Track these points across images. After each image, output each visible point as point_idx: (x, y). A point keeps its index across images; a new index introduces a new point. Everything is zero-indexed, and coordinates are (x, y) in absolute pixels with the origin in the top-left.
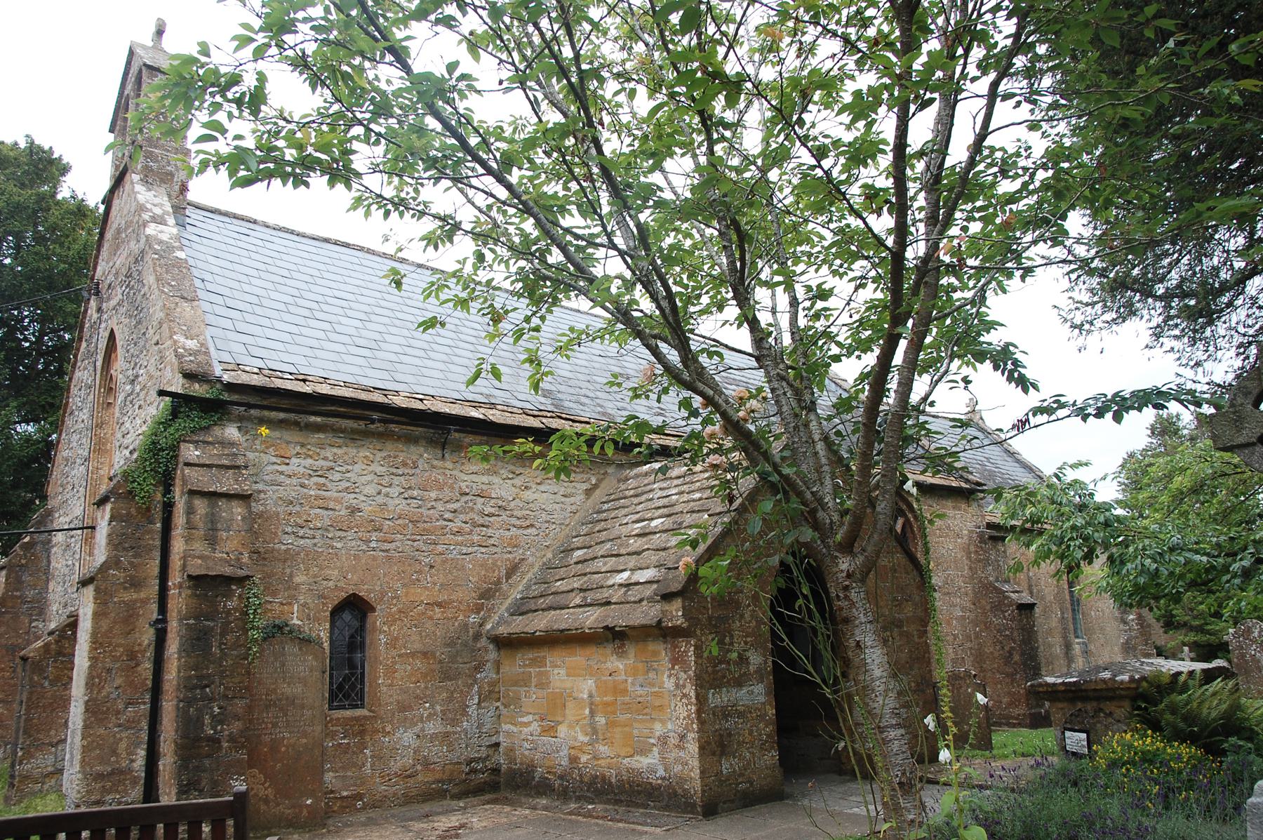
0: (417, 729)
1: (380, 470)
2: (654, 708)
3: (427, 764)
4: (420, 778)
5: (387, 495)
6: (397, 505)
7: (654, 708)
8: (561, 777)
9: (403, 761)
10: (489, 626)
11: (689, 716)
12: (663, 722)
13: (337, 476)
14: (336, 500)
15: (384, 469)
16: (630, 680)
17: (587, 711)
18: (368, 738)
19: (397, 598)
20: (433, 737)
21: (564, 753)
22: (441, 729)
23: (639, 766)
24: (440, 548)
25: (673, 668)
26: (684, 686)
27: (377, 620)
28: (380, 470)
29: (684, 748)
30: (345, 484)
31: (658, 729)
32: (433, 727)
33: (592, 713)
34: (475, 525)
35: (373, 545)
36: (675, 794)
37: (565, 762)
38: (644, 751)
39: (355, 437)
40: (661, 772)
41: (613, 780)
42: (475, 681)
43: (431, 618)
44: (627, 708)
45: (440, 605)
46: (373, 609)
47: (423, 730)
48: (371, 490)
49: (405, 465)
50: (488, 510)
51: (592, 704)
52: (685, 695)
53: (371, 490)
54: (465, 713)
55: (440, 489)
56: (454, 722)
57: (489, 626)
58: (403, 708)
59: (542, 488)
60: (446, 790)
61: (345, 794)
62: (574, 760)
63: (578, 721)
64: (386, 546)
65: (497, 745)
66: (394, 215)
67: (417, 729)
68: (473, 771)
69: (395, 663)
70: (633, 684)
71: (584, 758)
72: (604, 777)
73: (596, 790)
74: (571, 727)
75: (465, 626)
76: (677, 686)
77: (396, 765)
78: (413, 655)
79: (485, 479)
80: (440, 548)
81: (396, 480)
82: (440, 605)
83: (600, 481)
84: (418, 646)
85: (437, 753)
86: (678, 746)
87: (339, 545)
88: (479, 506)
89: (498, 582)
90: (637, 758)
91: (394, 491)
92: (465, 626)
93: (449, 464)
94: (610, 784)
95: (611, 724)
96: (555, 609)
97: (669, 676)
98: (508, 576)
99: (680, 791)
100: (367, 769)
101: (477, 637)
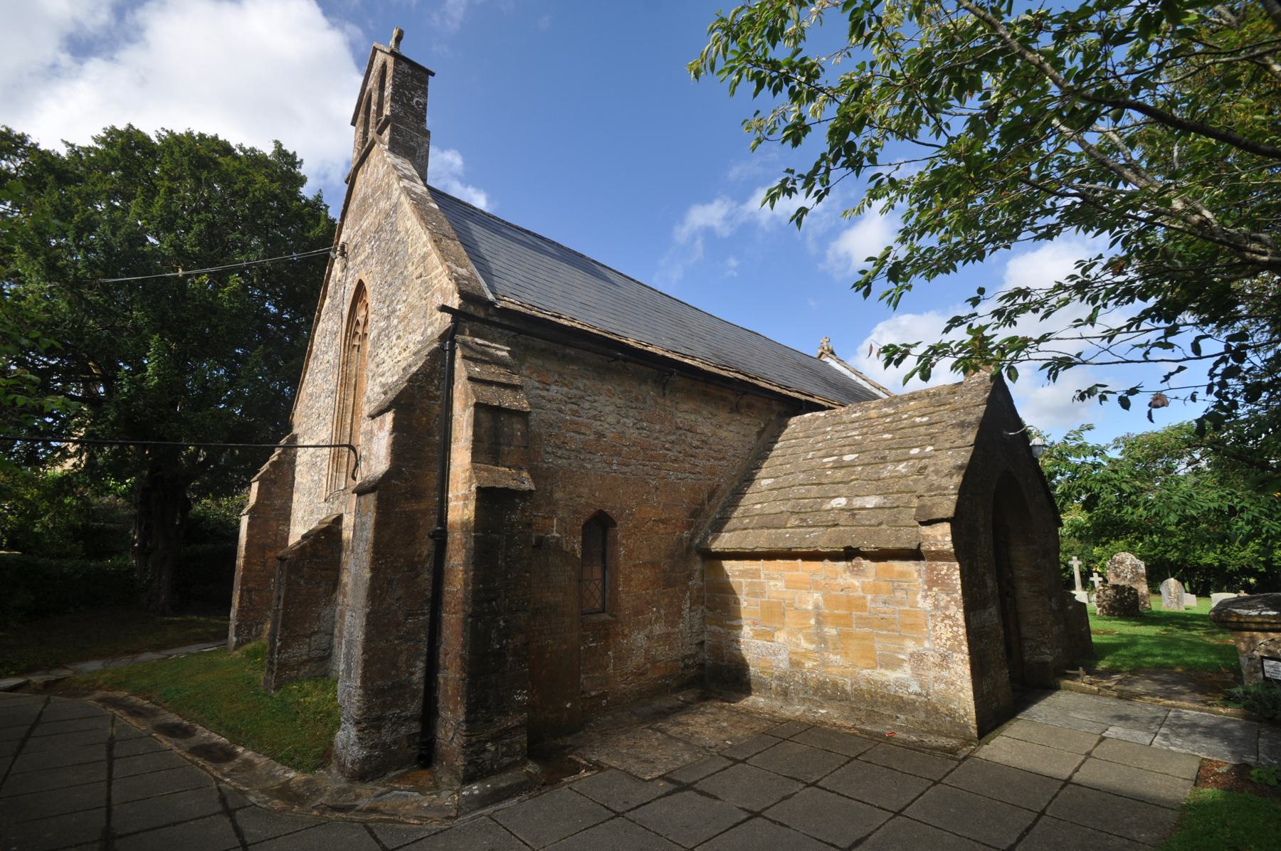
0: (647, 631)
1: (619, 402)
2: (905, 626)
3: (654, 661)
4: (650, 675)
5: (624, 424)
6: (633, 433)
7: (905, 626)
8: (780, 678)
9: (637, 660)
10: (697, 541)
11: (955, 638)
12: (918, 641)
13: (587, 405)
14: (587, 426)
15: (621, 402)
16: (869, 597)
17: (813, 622)
18: (611, 641)
19: (632, 514)
20: (660, 637)
21: (783, 656)
22: (664, 630)
23: (884, 679)
24: (663, 473)
25: (930, 589)
26: (946, 608)
27: (620, 533)
28: (619, 402)
29: (948, 668)
30: (593, 412)
31: (910, 646)
32: (658, 629)
33: (819, 623)
34: (687, 455)
35: (615, 467)
36: (936, 711)
37: (784, 665)
38: (893, 664)
39: (602, 372)
40: (915, 687)
41: (848, 688)
42: (688, 588)
43: (657, 533)
44: (864, 622)
45: (663, 521)
46: (614, 524)
47: (651, 632)
48: (611, 419)
49: (637, 400)
50: (695, 443)
51: (819, 615)
52: (949, 617)
53: (611, 419)
54: (681, 616)
55: (662, 423)
56: (673, 624)
57: (697, 541)
58: (638, 612)
59: (731, 428)
60: (668, 685)
61: (593, 693)
62: (795, 664)
63: (801, 629)
64: (625, 469)
65: (702, 643)
66: (766, 92)
67: (647, 631)
68: (687, 666)
69: (631, 572)
70: (873, 600)
71: (809, 664)
72: (835, 685)
73: (824, 695)
74: (791, 634)
75: (680, 540)
76: (936, 607)
77: (631, 665)
78: (644, 565)
79: (693, 417)
80: (663, 473)
81: (631, 412)
82: (663, 521)
83: (766, 425)
84: (647, 558)
85: (661, 651)
86: (940, 666)
87: (589, 466)
88: (689, 440)
89: (703, 504)
90: (879, 670)
91: (630, 422)
92: (680, 540)
93: (668, 403)
94: (844, 691)
95: (843, 636)
96: (768, 528)
97: (925, 597)
98: (709, 499)
99: (943, 710)
100: (610, 670)
101: (689, 549)
